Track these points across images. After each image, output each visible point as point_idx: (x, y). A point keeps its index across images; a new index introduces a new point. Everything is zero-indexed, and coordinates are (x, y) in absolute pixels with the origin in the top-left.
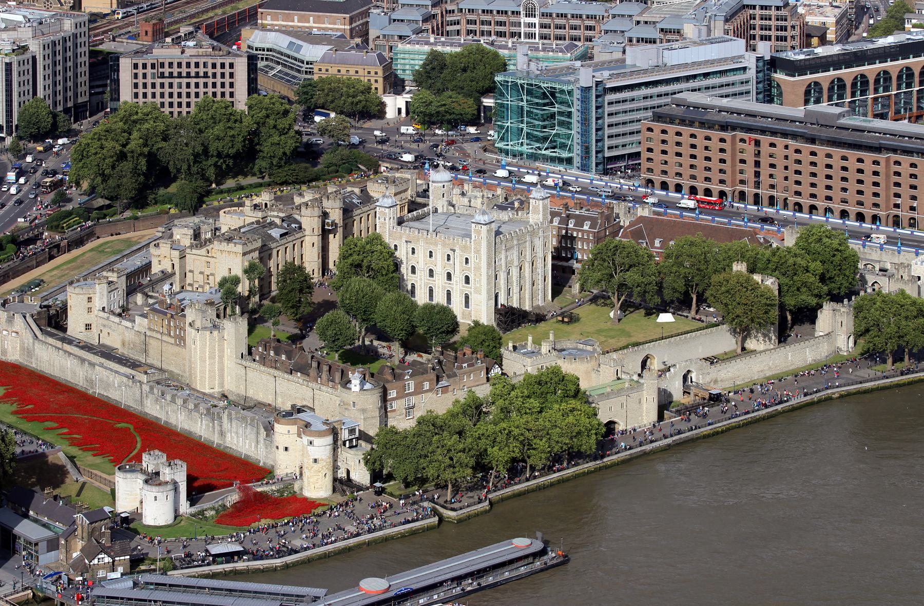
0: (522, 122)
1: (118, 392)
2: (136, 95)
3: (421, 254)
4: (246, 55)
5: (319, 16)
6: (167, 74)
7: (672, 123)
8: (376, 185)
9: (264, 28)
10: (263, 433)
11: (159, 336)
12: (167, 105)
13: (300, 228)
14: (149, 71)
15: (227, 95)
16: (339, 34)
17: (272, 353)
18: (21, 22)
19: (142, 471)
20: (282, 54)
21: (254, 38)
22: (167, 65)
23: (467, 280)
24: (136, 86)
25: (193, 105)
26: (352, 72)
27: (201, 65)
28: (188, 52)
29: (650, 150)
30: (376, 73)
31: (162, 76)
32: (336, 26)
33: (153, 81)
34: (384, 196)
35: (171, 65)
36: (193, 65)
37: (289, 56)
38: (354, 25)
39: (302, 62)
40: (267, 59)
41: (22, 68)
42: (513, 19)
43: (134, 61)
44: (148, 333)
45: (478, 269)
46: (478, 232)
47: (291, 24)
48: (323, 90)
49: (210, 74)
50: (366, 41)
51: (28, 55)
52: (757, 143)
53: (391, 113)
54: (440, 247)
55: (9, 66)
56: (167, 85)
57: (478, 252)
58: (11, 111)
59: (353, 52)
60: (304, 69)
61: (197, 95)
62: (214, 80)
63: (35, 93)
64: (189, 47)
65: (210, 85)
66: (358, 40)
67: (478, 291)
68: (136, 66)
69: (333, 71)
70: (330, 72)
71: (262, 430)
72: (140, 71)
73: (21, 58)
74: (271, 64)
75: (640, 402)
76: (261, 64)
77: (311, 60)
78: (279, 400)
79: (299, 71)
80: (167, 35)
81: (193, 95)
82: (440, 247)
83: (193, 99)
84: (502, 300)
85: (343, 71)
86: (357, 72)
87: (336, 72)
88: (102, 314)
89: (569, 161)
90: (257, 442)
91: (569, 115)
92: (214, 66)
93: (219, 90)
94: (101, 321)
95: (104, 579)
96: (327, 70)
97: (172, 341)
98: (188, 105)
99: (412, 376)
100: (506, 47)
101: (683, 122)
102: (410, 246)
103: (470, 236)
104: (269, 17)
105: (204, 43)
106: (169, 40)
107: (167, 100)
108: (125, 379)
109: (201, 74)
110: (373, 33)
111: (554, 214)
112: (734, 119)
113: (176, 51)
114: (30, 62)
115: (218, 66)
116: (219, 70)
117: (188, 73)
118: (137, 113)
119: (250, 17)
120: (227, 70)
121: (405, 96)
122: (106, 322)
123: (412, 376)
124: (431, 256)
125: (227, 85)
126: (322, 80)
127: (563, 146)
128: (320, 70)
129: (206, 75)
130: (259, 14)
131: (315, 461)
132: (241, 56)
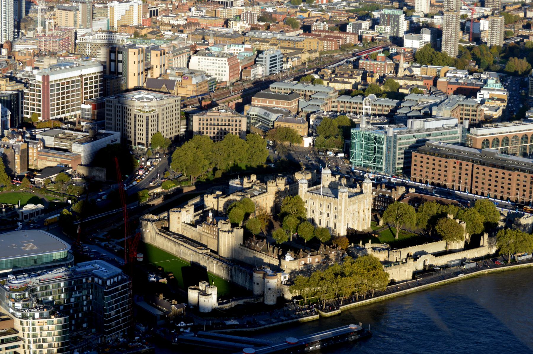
0: (362, 151)
1: (189, 257)
3: (317, 205)
7: (426, 154)
10: (249, 277)
11: (207, 234)
13: (267, 192)
14: (205, 122)
17: (253, 243)
19: (198, 289)
23: (336, 217)
27: (227, 121)
28: (223, 114)
29: (415, 165)
31: (211, 125)
34: (302, 179)
37: (264, 118)
42: (360, 106)
44: (202, 233)
45: (341, 212)
46: (341, 196)
52: (461, 164)
54: (325, 202)
55: (147, 118)
56: (212, 129)
57: (341, 204)
67: (340, 222)
68: (200, 120)
71: (248, 275)
75: (405, 271)
78: (256, 264)
82: (325, 202)
84: (350, 226)
88: (183, 224)
89: (381, 169)
90: (246, 281)
91: (382, 148)
94: (183, 227)
95: (183, 332)
97: (212, 237)
99: (311, 256)
100: (356, 118)
101: (430, 154)
102: (312, 201)
103: (337, 198)
104: (256, 101)
108: (192, 252)
111: (373, 191)
112: (451, 153)
113: (217, 114)
116: (234, 123)
120: (238, 123)
122: (185, 228)
123: (311, 256)
124: (321, 206)
127: (378, 162)
131: (270, 289)
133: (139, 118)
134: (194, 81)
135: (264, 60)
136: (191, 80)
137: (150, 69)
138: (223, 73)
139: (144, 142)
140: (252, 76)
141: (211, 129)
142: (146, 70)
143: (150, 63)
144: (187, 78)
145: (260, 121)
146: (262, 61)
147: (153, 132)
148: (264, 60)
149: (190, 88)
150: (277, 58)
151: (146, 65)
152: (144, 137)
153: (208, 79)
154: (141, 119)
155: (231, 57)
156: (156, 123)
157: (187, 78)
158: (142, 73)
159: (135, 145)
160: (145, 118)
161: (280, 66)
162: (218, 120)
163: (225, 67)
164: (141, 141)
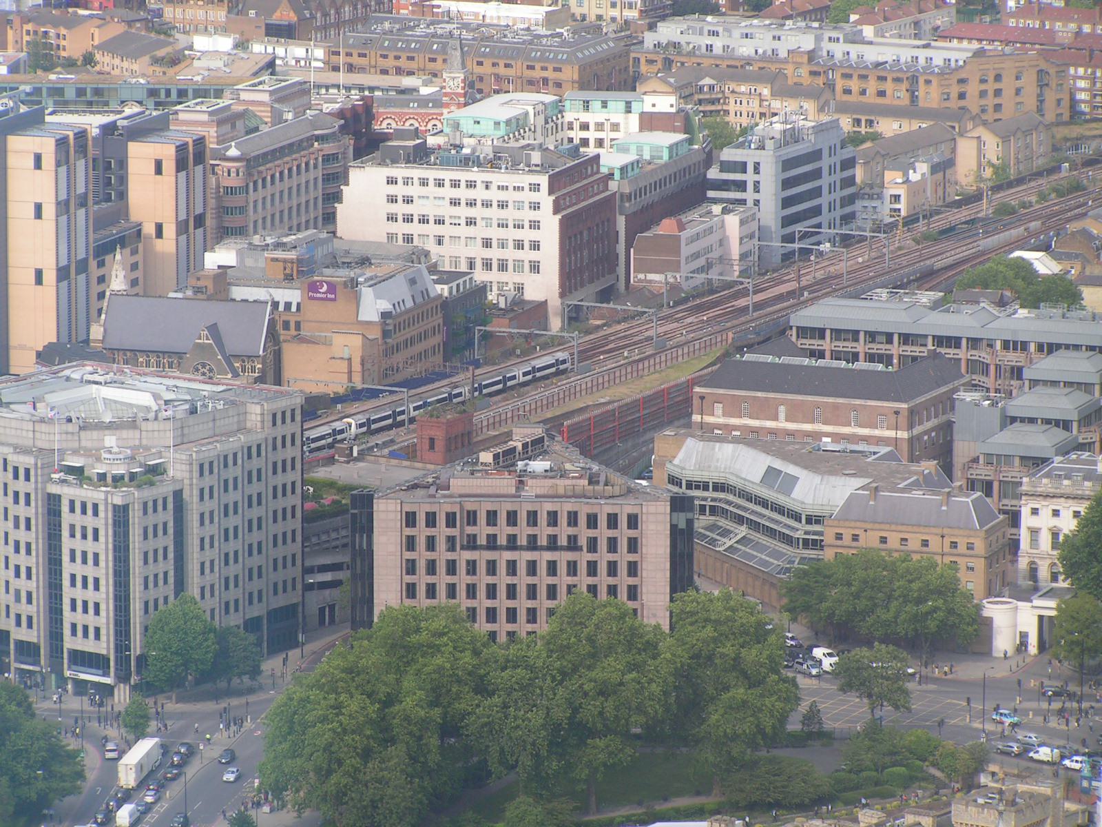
2: (411, 591)
4: (667, 496)
5: (836, 407)
6: (482, 541)
8: (972, 810)
9: (707, 433)
12: (482, 616)
14: (442, 531)
15: (623, 595)
16: (884, 450)
18: (148, 409)
20: (749, 497)
21: (689, 457)
22: (482, 518)
24: (411, 567)
25: (542, 616)
26: (914, 544)
28: (533, 488)
30: (970, 547)
31: (471, 544)
32: (877, 433)
33: (451, 556)
35: (492, 517)
36: (543, 519)
37: (764, 503)
38: (917, 430)
39: (797, 517)
40: (714, 510)
41: (151, 519)
43: (407, 508)
47: (770, 424)
48: (849, 584)
49: (583, 542)
50: (948, 469)
51: (163, 489)
53: (1003, 643)
55: (121, 515)
58: (128, 623)
59: (917, 494)
60: (799, 534)
61: (552, 592)
62: (591, 557)
63: (180, 585)
64: (534, 476)
65: (583, 568)
66: (929, 466)
68: (410, 519)
69: (870, 540)
70: (862, 542)
72: (421, 532)
73: (148, 494)
74: (723, 523)
76: (702, 522)
77: (817, 512)
79: (788, 540)
80: (486, 445)
81: (542, 592)
83: (543, 603)
85: (894, 541)
86: (925, 543)
87: (876, 544)
92: (592, 521)
93: (603, 580)
96: (855, 538)
98: (532, 615)
104: (719, 408)
105: (568, 466)
106: (486, 457)
107: (483, 603)
109: (563, 541)
110: (963, 450)
113: (506, 484)
114: (170, 506)
115: (603, 521)
116: (603, 533)
117: (533, 539)
118: (418, 630)
119: (674, 409)
121: (1037, 602)
125: (623, 569)
126: (845, 563)
128: (839, 537)
129: (573, 544)
130: (696, 402)
132: (657, 499)
133: (78, 519)
134: (372, 306)
135: (750, 177)
136: (357, 298)
137: (122, 242)
138: (527, 255)
139: (104, 646)
140: (685, 268)
141: (472, 567)
142: (103, 250)
143: (124, 212)
144: (332, 288)
145: (740, 520)
146: (741, 186)
147: (152, 594)
148: (750, 177)
149: (349, 345)
150: (825, 163)
151: (100, 223)
152: (105, 620)
153: (443, 290)
154: (89, 521)
155: (573, 176)
156: (169, 541)
157: (332, 288)
158: (83, 266)
159: (57, 669)
160: (104, 522)
161: (839, 213)
162: (512, 518)
163: (535, 225)
164: (90, 646)
